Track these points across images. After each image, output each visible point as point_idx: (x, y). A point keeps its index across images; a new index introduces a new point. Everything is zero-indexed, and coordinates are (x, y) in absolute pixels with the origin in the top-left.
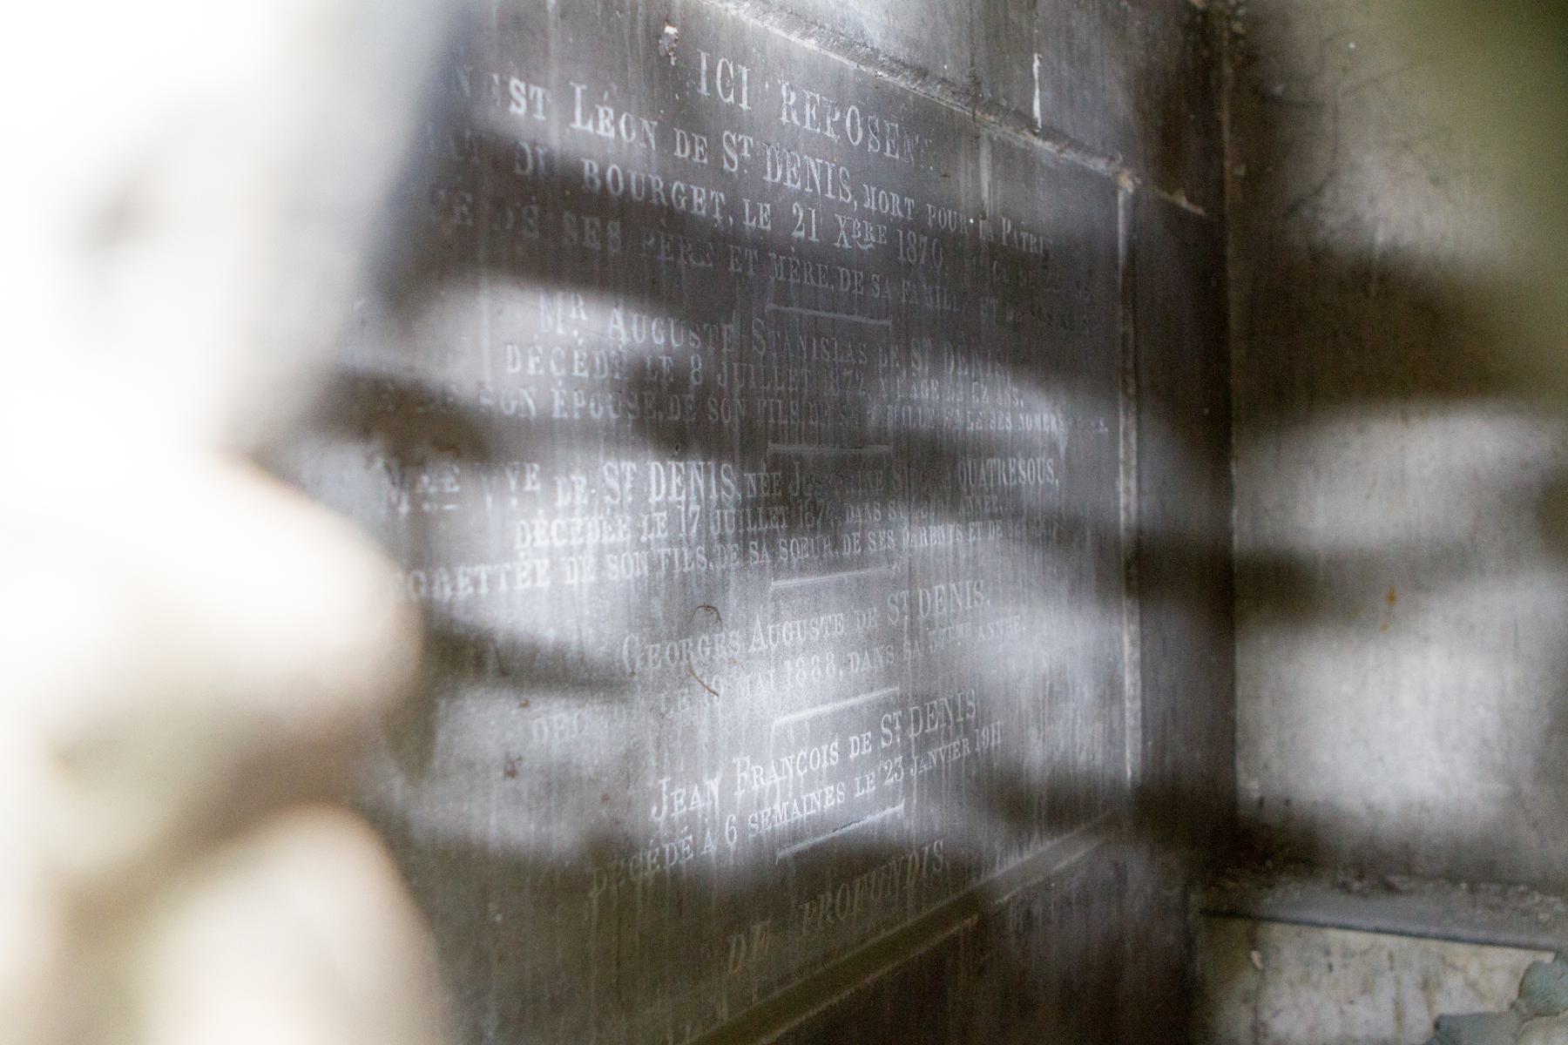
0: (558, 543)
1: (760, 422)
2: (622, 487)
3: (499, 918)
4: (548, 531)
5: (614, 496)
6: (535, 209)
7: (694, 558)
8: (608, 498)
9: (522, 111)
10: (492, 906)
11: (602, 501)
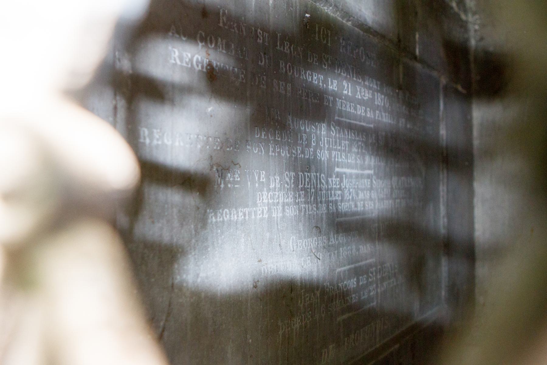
0: (270, 201)
1: (333, 159)
2: (290, 180)
3: (250, 341)
4: (268, 196)
5: (288, 185)
6: (265, 77)
7: (312, 209)
8: (286, 185)
9: (261, 41)
10: (248, 336)
11: (284, 186)
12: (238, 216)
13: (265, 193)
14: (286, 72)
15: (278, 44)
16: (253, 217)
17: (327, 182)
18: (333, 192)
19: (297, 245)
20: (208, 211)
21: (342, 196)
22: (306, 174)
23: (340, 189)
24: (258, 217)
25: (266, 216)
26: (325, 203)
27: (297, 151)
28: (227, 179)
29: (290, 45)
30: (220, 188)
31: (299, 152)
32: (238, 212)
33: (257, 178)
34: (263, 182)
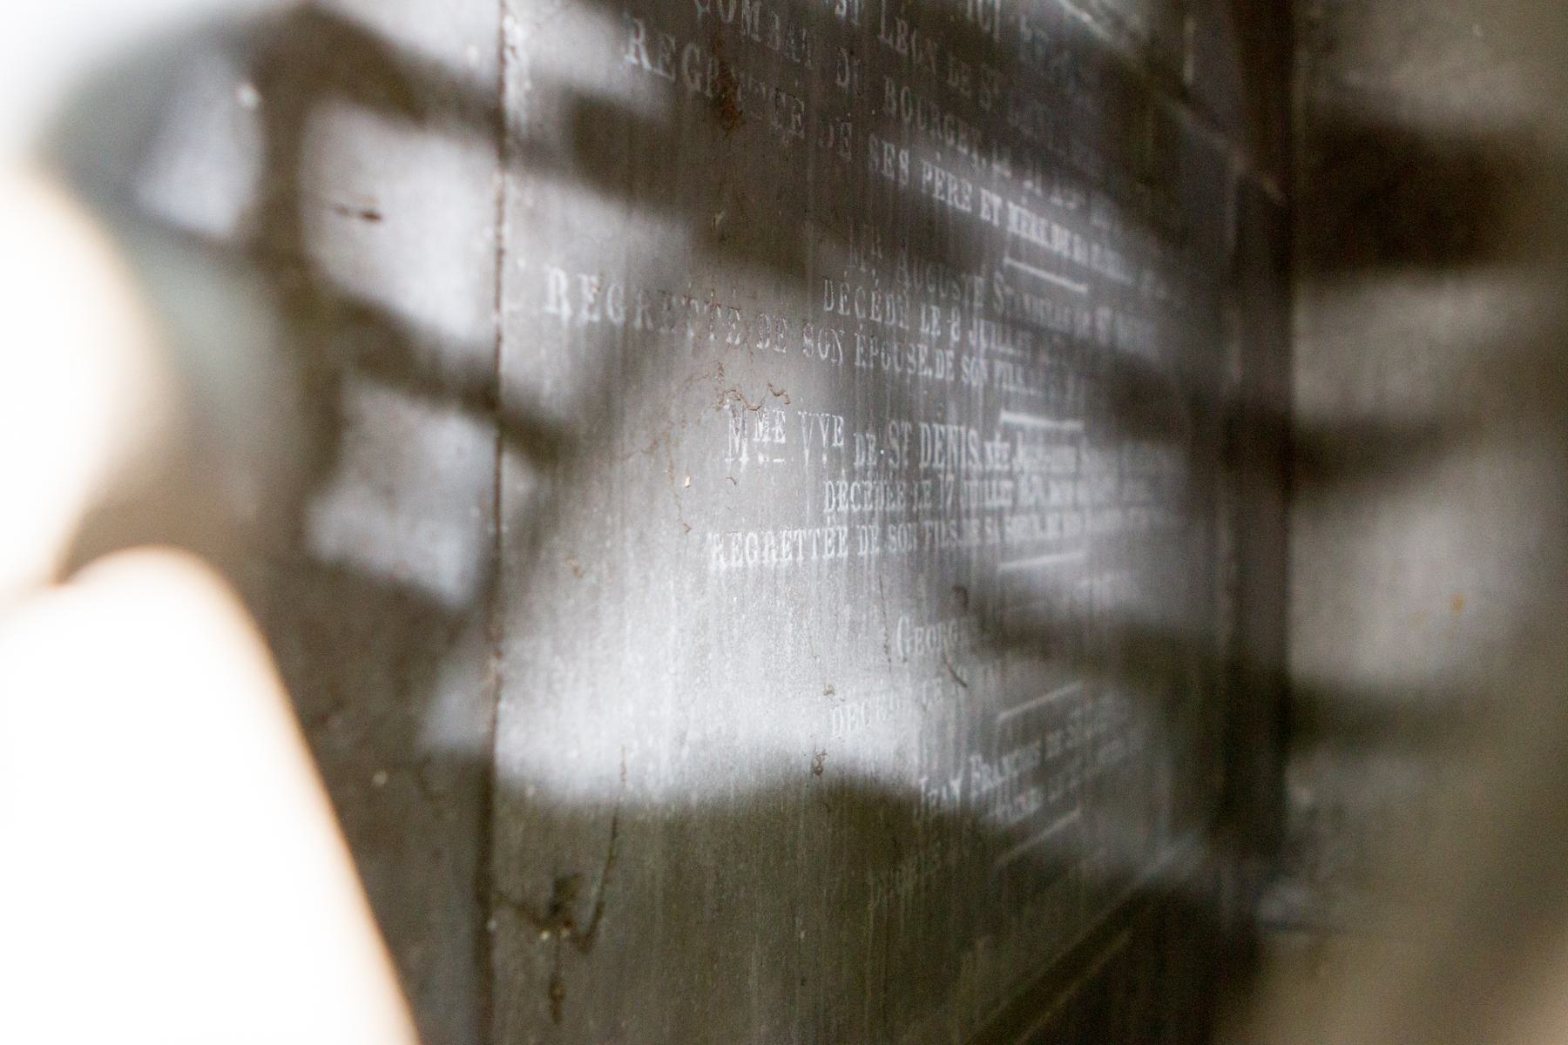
0: (855, 509)
1: (996, 385)
2: (901, 444)
3: (802, 935)
4: (848, 494)
5: (895, 460)
6: (850, 126)
7: (948, 535)
8: (891, 461)
9: (843, 13)
10: (799, 921)
11: (887, 464)
12: (779, 555)
13: (843, 483)
14: (899, 112)
15: (883, 27)
16: (814, 556)
17: (983, 456)
18: (994, 484)
19: (912, 643)
20: (709, 536)
21: (1015, 496)
22: (936, 426)
23: (1011, 475)
24: (827, 556)
25: (844, 554)
26: (978, 515)
27: (917, 358)
28: (756, 439)
29: (910, 32)
30: (739, 464)
31: (922, 360)
32: (779, 543)
33: (825, 437)
34: (839, 449)
